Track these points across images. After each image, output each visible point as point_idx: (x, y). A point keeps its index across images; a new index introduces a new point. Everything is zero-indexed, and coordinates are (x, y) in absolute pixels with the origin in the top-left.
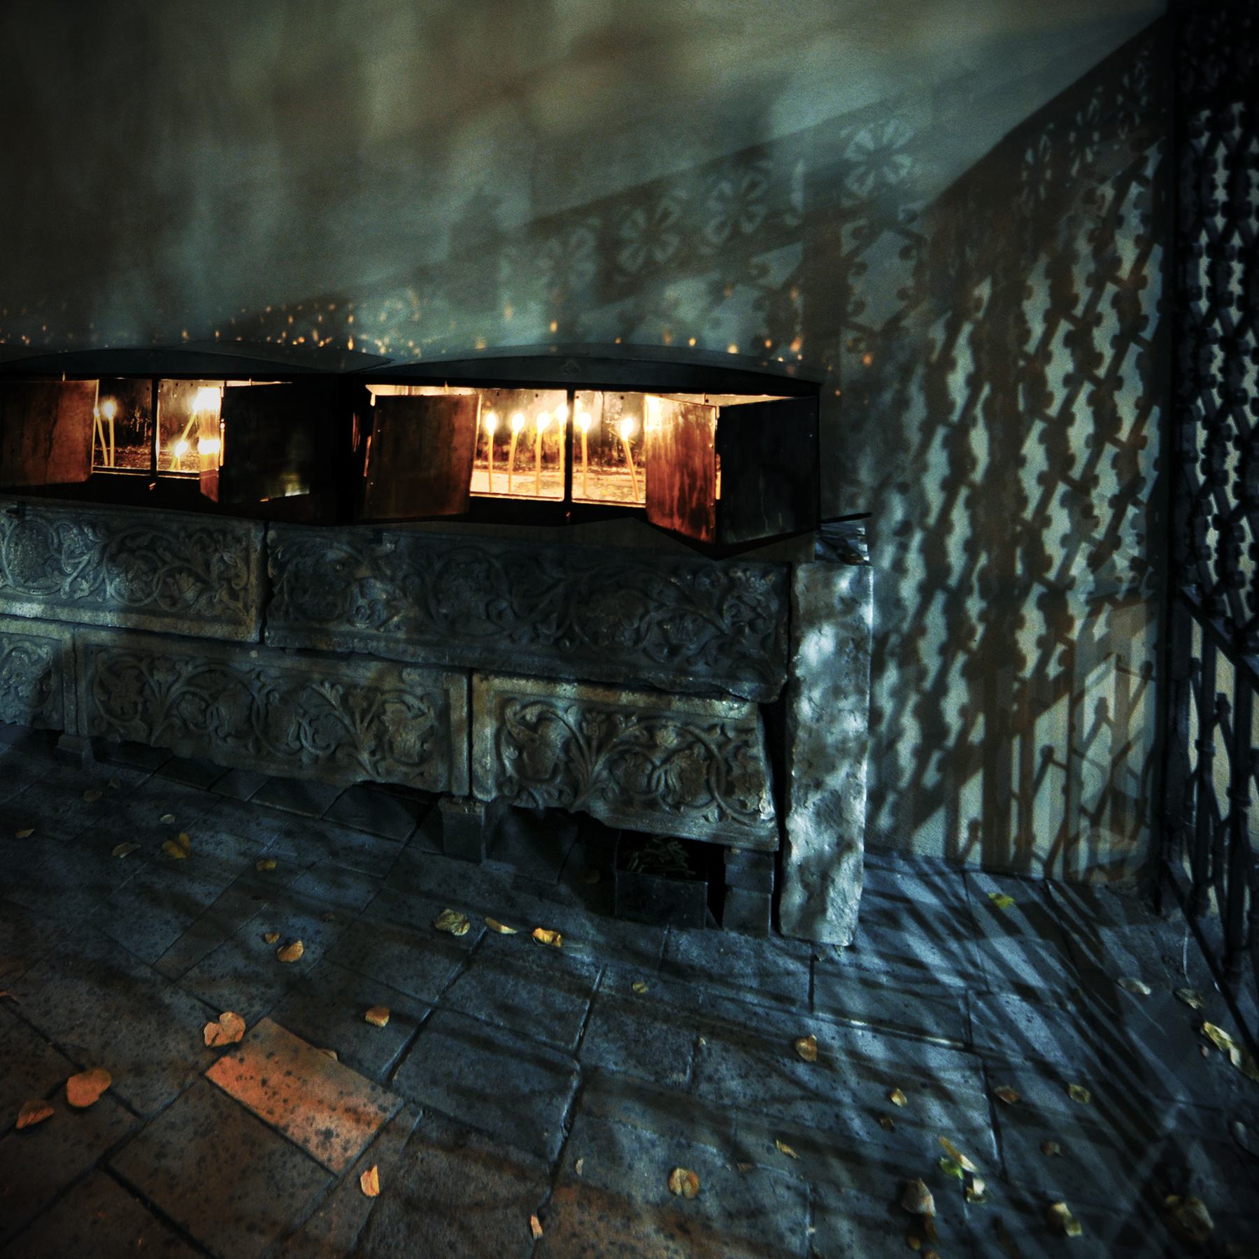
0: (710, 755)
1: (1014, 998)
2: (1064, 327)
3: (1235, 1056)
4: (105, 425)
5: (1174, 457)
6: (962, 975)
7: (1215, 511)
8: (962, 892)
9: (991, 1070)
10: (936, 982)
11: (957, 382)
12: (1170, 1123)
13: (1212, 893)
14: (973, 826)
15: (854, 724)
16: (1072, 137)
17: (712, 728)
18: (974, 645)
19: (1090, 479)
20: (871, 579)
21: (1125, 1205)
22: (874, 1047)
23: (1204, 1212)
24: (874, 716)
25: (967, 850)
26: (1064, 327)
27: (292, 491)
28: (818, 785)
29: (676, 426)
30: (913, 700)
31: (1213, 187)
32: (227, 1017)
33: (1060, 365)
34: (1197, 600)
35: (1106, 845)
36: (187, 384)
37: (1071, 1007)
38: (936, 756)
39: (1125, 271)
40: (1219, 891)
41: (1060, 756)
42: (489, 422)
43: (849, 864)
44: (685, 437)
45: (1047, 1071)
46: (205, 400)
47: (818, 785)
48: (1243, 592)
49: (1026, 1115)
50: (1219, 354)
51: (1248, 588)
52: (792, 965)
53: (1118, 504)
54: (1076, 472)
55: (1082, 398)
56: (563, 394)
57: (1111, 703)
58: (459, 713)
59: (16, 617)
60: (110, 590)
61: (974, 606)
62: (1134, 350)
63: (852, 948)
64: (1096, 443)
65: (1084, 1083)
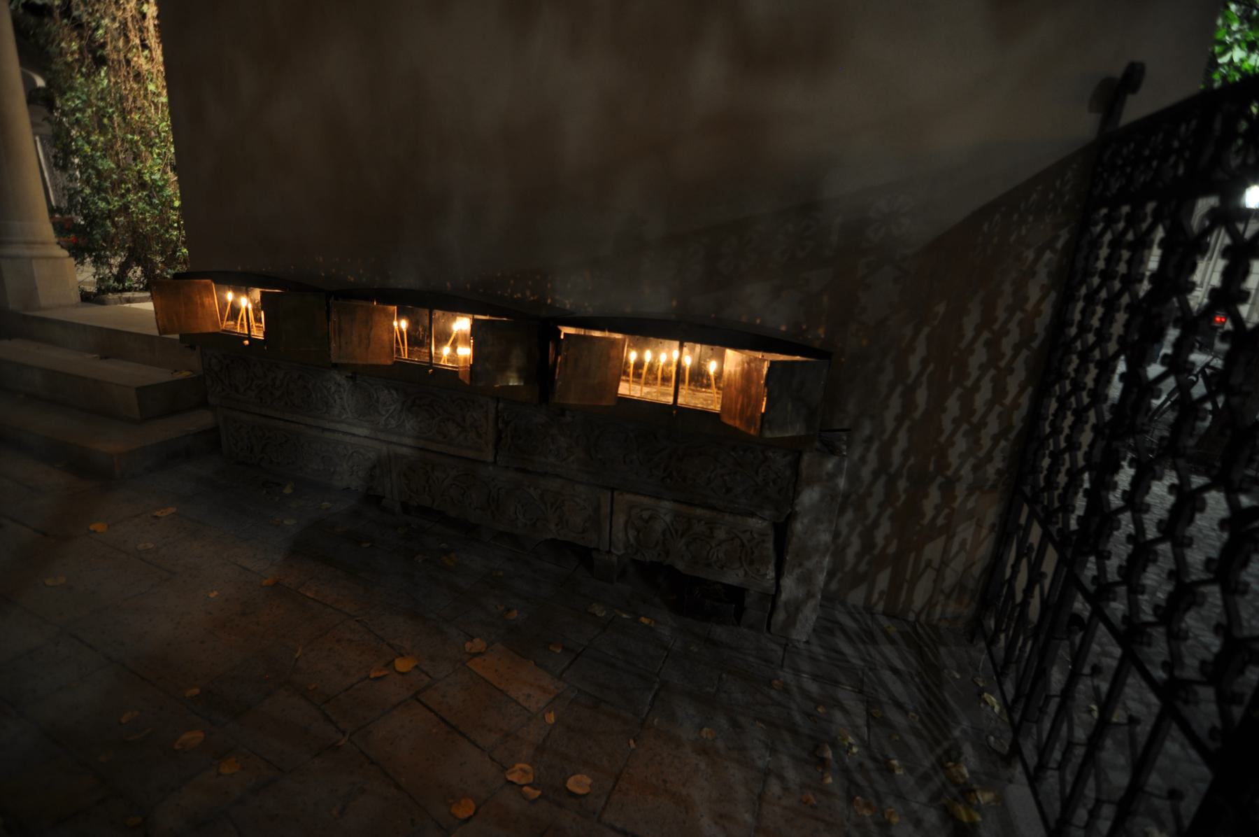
0: (743, 545)
1: (888, 673)
2: (986, 335)
3: (997, 709)
4: (401, 333)
5: (1035, 415)
6: (864, 660)
7: (1052, 448)
8: (870, 623)
9: (871, 703)
10: (848, 662)
11: (914, 362)
12: (957, 733)
13: (1002, 636)
14: (881, 593)
15: (825, 537)
16: (1015, 217)
17: (745, 531)
18: (899, 504)
19: (983, 423)
20: (846, 464)
21: (927, 764)
22: (813, 687)
23: (965, 771)
24: (836, 535)
25: (876, 604)
26: (986, 335)
27: (513, 382)
28: (800, 565)
29: (743, 369)
30: (859, 528)
31: (1097, 259)
32: (477, 640)
33: (980, 356)
34: (1029, 494)
35: (952, 608)
36: (450, 314)
37: (917, 679)
38: (867, 558)
39: (1030, 306)
40: (1007, 637)
41: (936, 564)
42: (633, 356)
43: (811, 604)
44: (747, 375)
45: (899, 706)
46: (462, 324)
47: (800, 565)
48: (1056, 493)
49: (885, 723)
50: (1075, 361)
51: (1060, 491)
52: (774, 646)
53: (996, 439)
54: (975, 419)
55: (987, 378)
56: (676, 343)
57: (969, 542)
58: (605, 510)
59: (354, 435)
60: (408, 426)
61: (902, 484)
62: (1025, 353)
63: (807, 642)
64: (991, 404)
65: (917, 712)
